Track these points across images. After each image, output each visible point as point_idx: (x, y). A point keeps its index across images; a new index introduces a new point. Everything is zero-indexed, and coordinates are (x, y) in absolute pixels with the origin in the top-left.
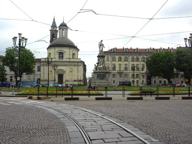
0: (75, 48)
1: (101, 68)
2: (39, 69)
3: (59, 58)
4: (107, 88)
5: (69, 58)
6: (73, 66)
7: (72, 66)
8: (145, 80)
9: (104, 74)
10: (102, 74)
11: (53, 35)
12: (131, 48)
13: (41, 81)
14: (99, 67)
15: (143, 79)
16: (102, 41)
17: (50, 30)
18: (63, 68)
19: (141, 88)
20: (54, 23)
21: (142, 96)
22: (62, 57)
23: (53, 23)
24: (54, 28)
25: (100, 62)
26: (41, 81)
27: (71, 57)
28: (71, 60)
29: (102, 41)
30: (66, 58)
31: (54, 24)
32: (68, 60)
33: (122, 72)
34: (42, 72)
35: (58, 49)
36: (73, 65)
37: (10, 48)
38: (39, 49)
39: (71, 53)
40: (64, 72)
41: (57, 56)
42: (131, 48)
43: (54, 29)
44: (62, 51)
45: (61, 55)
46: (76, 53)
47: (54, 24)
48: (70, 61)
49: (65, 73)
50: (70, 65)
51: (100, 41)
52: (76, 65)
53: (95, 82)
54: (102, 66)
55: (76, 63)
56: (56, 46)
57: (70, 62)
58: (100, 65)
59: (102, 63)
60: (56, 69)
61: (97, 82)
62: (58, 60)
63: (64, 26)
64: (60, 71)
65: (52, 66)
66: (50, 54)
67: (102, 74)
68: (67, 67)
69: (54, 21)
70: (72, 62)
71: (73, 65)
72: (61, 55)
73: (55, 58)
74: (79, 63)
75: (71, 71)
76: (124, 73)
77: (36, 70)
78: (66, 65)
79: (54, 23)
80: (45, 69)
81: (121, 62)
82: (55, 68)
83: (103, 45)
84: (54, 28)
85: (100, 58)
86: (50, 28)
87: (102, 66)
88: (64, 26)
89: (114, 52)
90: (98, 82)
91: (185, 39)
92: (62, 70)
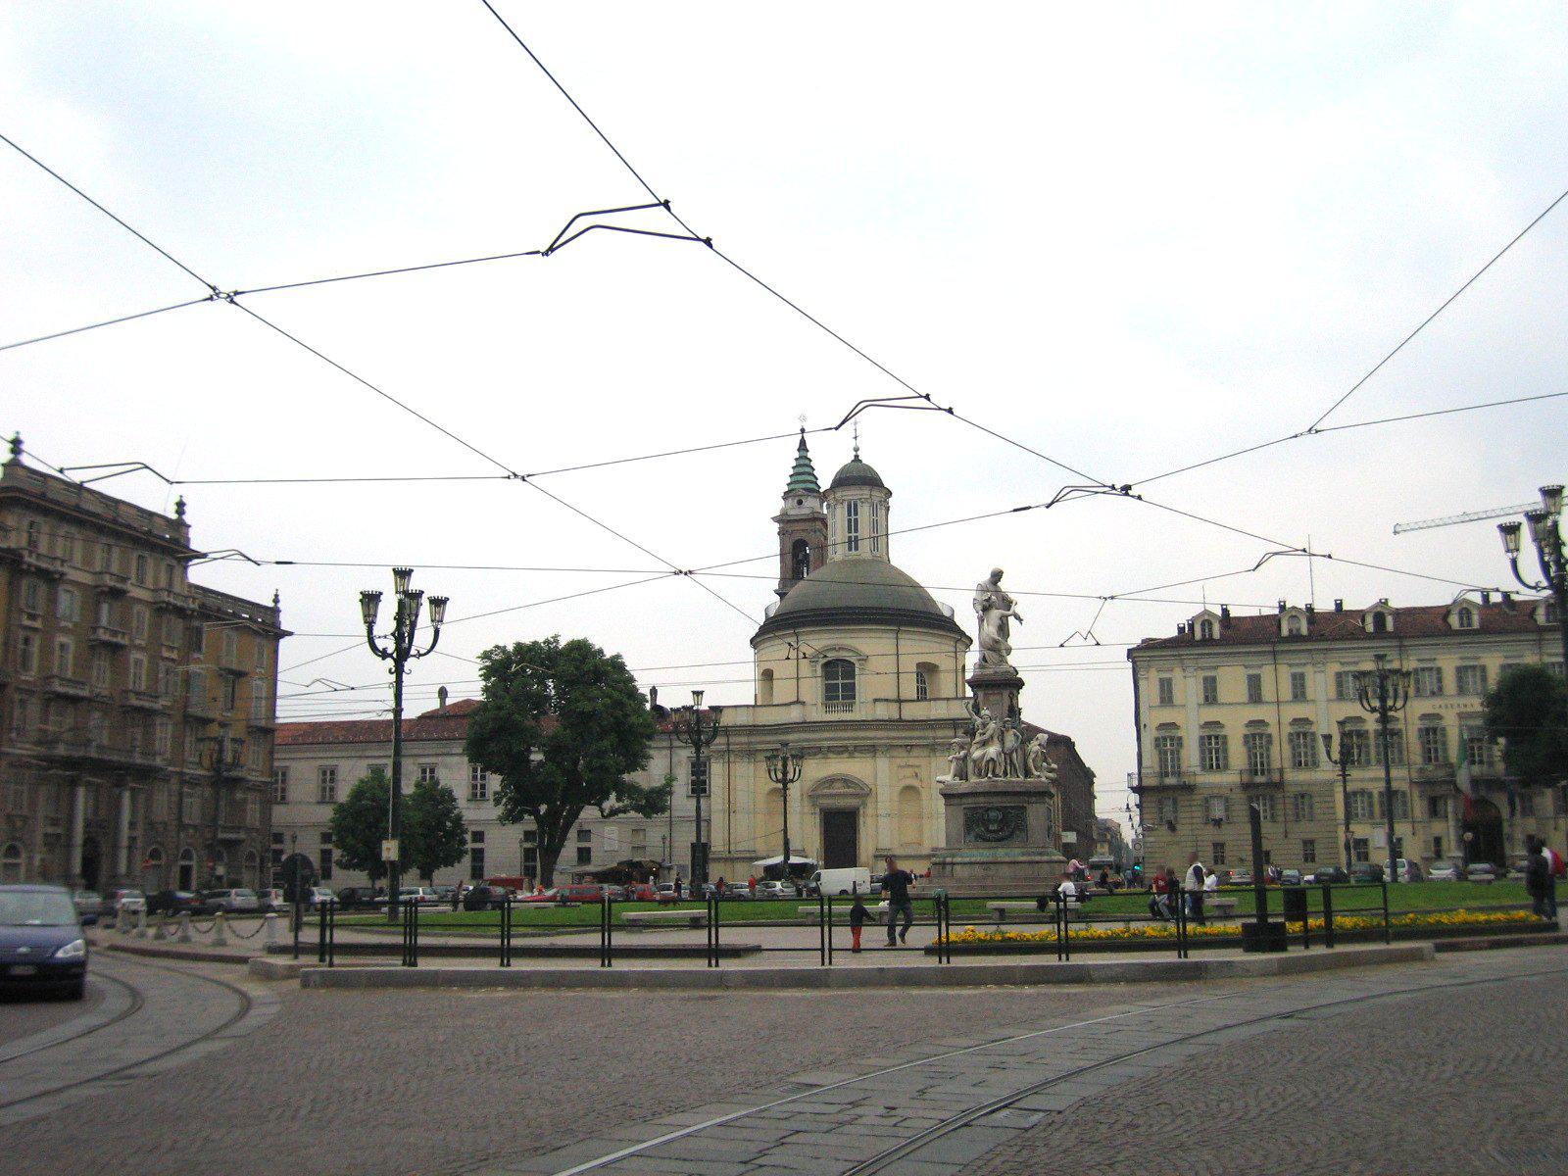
0: (940, 627)
1: (991, 766)
2: (479, 782)
3: (828, 698)
4: (952, 904)
5: (894, 696)
6: (926, 752)
7: (915, 752)
8: (1452, 832)
9: (1008, 802)
10: (996, 801)
11: (800, 546)
12: (1339, 605)
13: (714, 860)
14: (977, 754)
15: (1438, 828)
16: (997, 576)
17: (190, 526)
18: (856, 767)
19: (826, 907)
20: (803, 467)
21: (1071, 956)
22: (850, 692)
23: (797, 470)
24: (800, 502)
25: (984, 725)
26: (714, 860)
27: (910, 689)
28: (912, 711)
29: (997, 576)
30: (876, 700)
31: (800, 478)
32: (882, 712)
33: (1276, 777)
34: (720, 800)
35: (817, 641)
36: (921, 742)
37: (503, 649)
38: (694, 640)
39: (909, 665)
40: (864, 793)
41: (813, 689)
42: (1339, 605)
43: (805, 511)
44: (843, 655)
45: (839, 677)
46: (945, 663)
47: (800, 478)
48: (900, 720)
49: (870, 801)
50: (900, 742)
51: (986, 577)
52: (942, 745)
53: (949, 860)
54: (992, 750)
55: (940, 733)
56: (804, 625)
57: (900, 723)
58: (984, 744)
59: (992, 725)
60: (790, 776)
61: (959, 860)
62: (817, 714)
63: (860, 479)
64: (838, 788)
65: (768, 754)
66: (768, 676)
67: (996, 801)
68: (883, 764)
69: (803, 453)
70: (914, 724)
71: (925, 742)
72: (839, 677)
73: (798, 702)
74: (732, 739)
75: (909, 789)
76: (1291, 790)
77: (456, 794)
78: (872, 750)
79: (803, 467)
80: (739, 786)
81: (1265, 707)
82: (785, 773)
83: (1007, 603)
84: (800, 502)
85: (985, 694)
86: (777, 506)
87: (992, 750)
88: (860, 479)
89: (1208, 641)
90: (967, 860)
91: (1510, 530)
92: (846, 781)
